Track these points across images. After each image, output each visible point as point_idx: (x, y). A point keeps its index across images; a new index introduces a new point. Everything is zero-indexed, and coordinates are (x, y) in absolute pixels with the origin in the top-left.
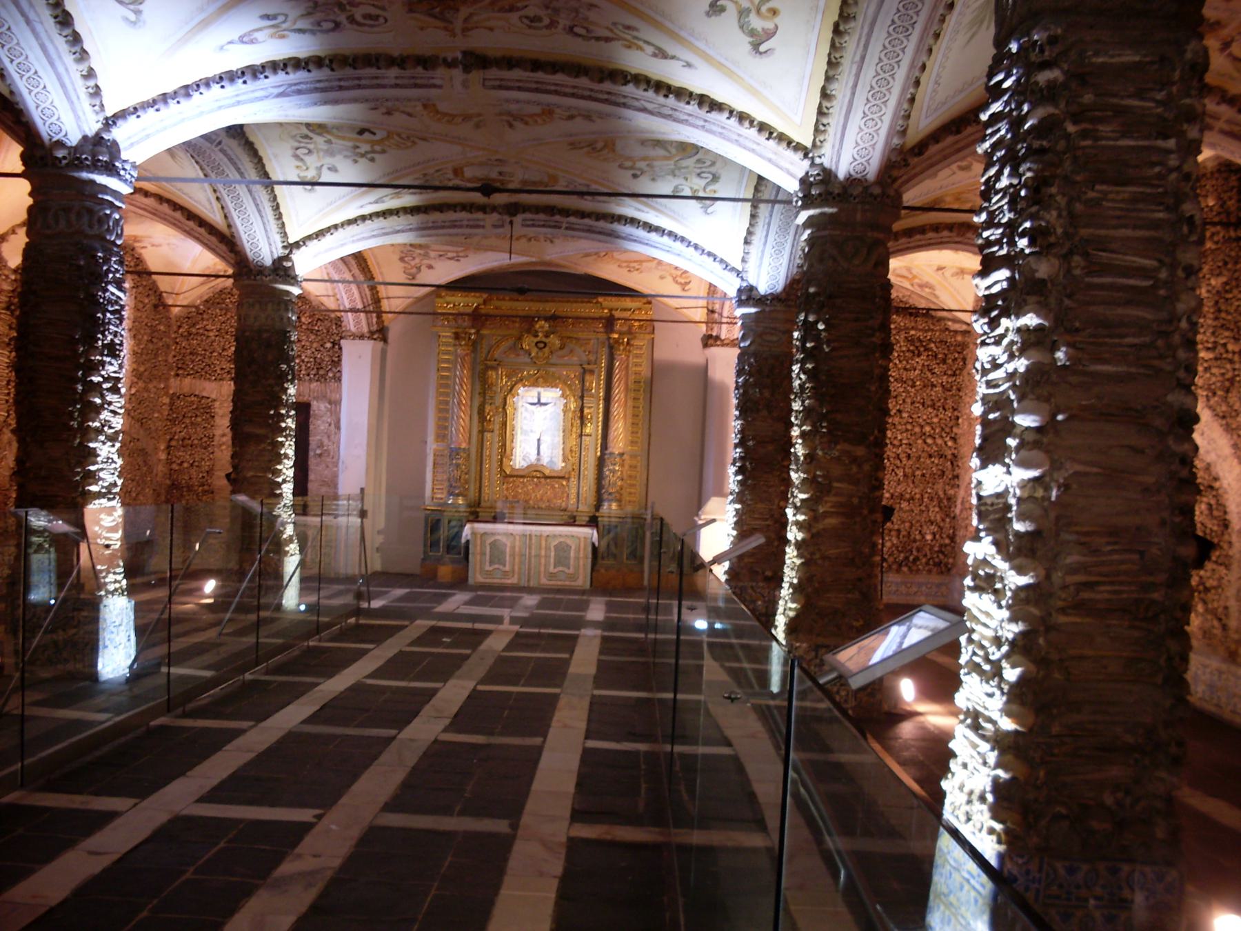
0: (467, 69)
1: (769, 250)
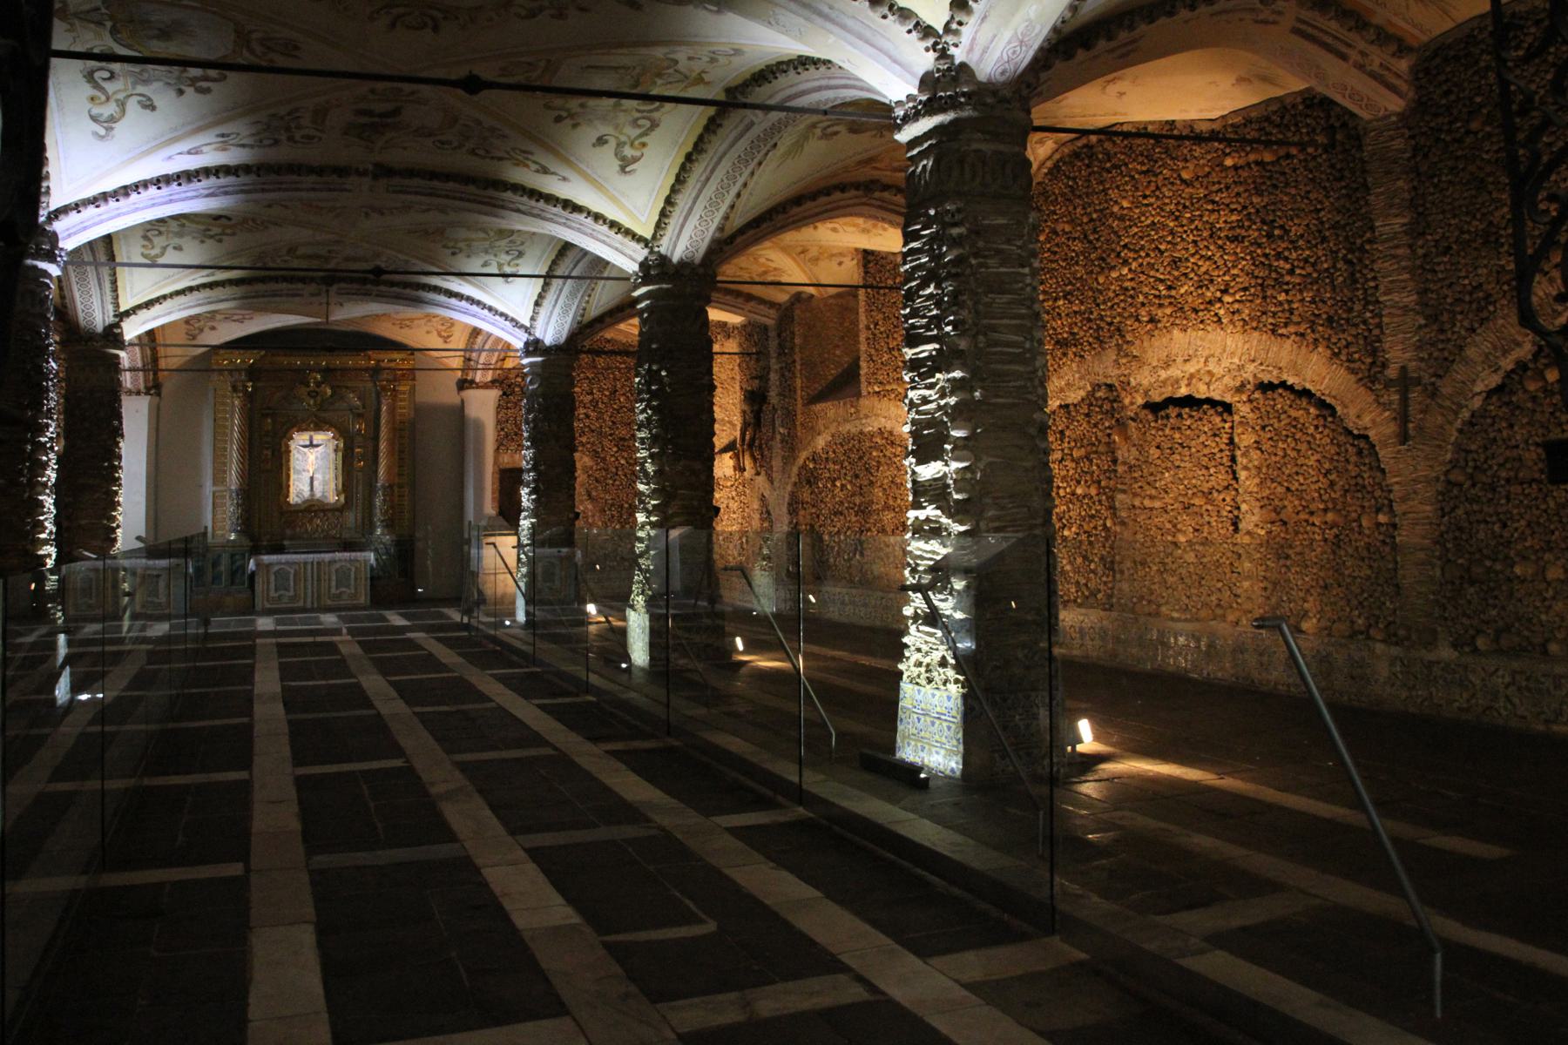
0: (375, 177)
1: (558, 310)
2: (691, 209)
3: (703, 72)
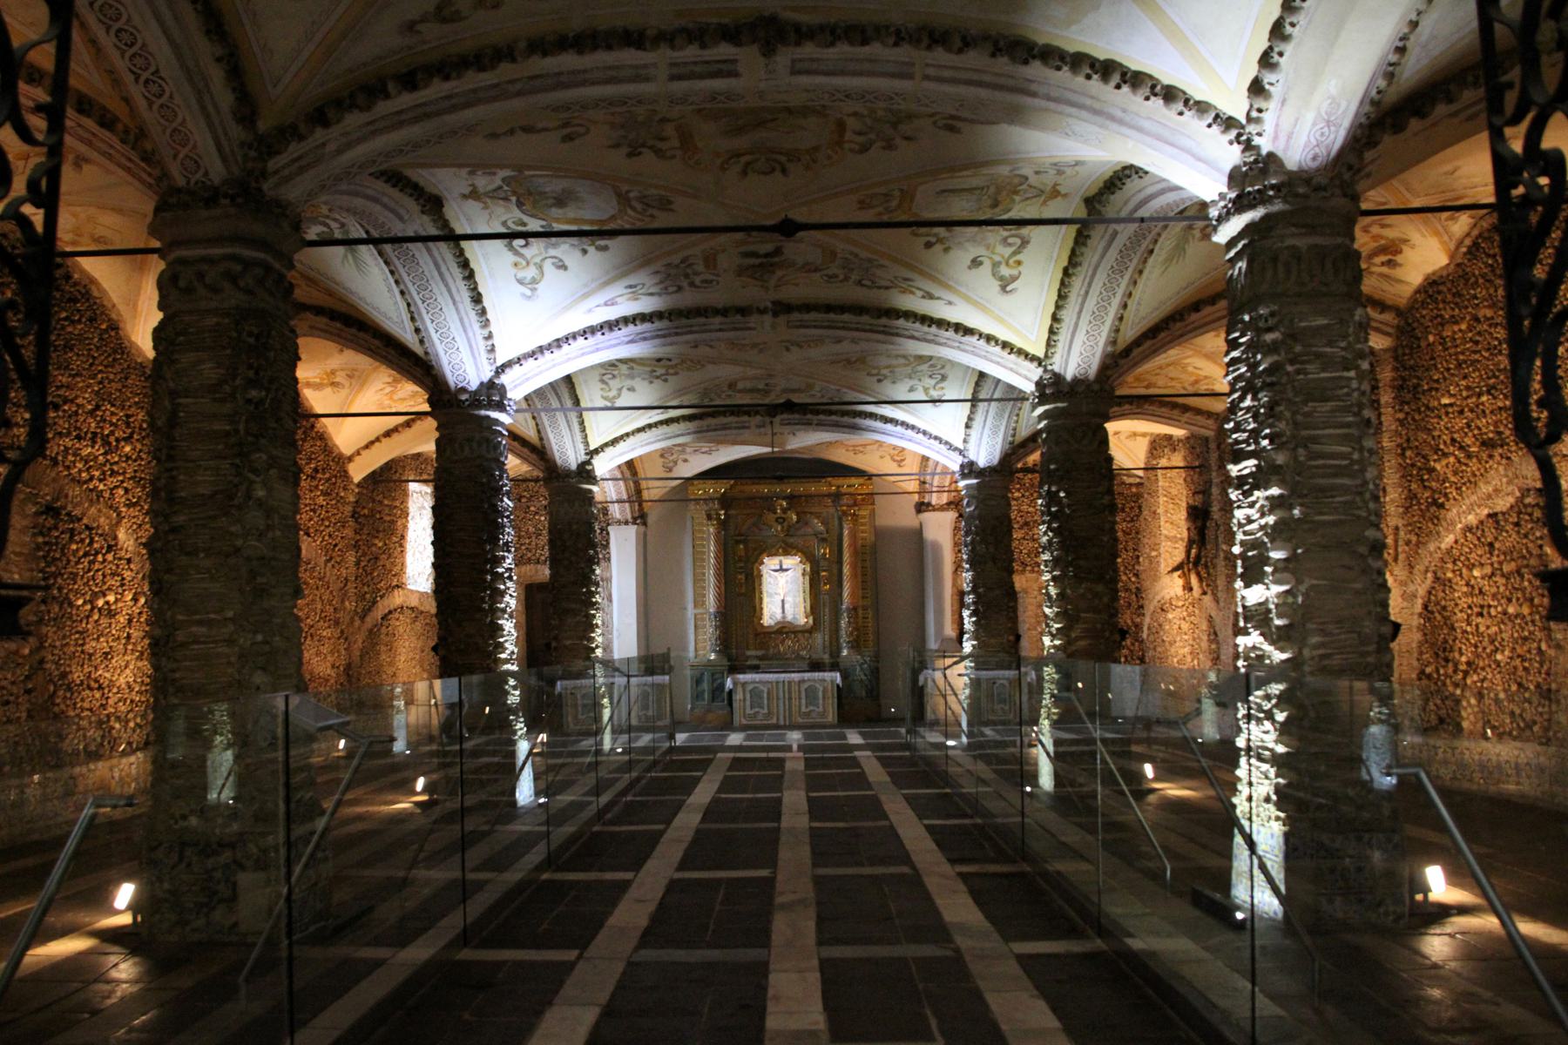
0: (775, 314)
1: (987, 431)
2: (1076, 325)
3: (1056, 185)
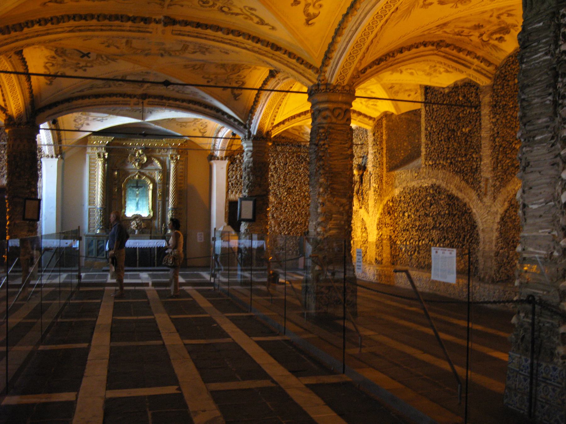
0: (166, 24)
